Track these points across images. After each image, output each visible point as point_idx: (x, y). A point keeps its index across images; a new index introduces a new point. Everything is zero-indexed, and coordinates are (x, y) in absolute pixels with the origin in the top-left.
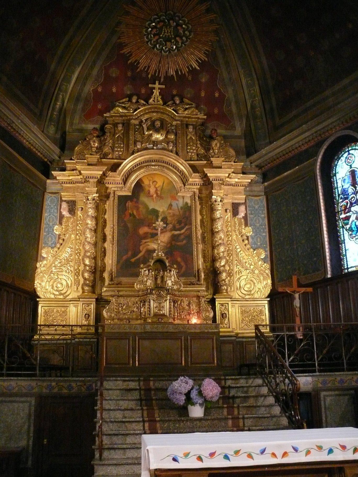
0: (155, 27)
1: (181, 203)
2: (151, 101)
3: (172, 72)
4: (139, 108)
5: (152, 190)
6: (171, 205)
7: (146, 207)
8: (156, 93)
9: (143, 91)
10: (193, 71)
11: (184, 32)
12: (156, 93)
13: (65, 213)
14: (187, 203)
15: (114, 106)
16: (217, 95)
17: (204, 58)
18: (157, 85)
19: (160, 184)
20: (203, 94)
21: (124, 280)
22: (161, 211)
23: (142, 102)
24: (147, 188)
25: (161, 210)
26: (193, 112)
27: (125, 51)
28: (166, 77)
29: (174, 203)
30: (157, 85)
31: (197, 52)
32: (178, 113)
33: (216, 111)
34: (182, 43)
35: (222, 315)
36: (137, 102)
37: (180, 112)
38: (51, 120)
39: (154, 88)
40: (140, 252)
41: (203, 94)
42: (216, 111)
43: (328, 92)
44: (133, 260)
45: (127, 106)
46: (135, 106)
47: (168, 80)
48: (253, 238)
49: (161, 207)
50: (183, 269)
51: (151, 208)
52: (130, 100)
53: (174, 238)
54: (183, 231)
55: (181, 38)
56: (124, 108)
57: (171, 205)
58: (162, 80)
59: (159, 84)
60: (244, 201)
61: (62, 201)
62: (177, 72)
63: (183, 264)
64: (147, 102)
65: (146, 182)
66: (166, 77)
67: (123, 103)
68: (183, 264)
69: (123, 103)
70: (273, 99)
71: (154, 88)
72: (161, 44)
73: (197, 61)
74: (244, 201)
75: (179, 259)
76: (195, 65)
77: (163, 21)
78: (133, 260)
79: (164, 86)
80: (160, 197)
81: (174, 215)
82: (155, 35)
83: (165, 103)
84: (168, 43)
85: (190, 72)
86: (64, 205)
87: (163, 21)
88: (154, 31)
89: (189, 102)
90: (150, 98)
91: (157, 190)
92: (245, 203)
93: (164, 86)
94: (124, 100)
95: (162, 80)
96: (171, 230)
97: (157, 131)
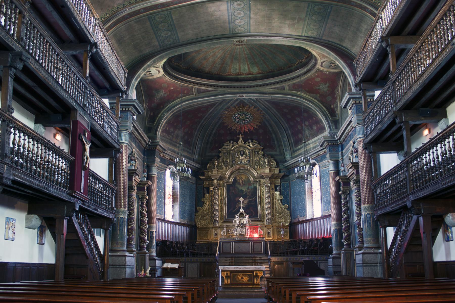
0: (237, 117)
1: (253, 186)
2: (239, 142)
3: (246, 130)
4: (234, 146)
5: (241, 182)
6: (248, 188)
7: (238, 189)
8: (241, 139)
9: (235, 138)
10: (255, 129)
11: (249, 117)
12: (241, 139)
13: (206, 192)
14: (255, 186)
15: (223, 145)
16: (268, 137)
17: (259, 124)
18: (241, 136)
19: (244, 179)
20: (261, 138)
21: (230, 219)
22: (244, 190)
23: (235, 143)
24: (238, 181)
25: (244, 190)
26: (257, 145)
27: (226, 124)
28: (244, 132)
29: (250, 187)
30: (241, 136)
31: (256, 123)
32: (250, 147)
33: (268, 144)
34: (249, 120)
35: (268, 233)
36: (233, 143)
37: (251, 145)
38: (197, 153)
39: (240, 137)
40: (236, 208)
41: (261, 138)
42: (268, 144)
43: (310, 141)
44: (233, 211)
45: (229, 145)
46: (231, 145)
47: (245, 134)
48: (283, 200)
49: (244, 189)
50: (254, 214)
51: (240, 189)
52: (230, 143)
53: (250, 202)
54: (253, 199)
55: (248, 119)
56: (228, 146)
57: (248, 188)
58: (243, 133)
59: (242, 135)
60: (280, 184)
61: (204, 188)
62: (249, 130)
63: (253, 212)
64: (237, 142)
65: (238, 178)
66: (244, 132)
67: (227, 144)
68: (253, 212)
69: (227, 144)
70: (292, 139)
71: (240, 137)
72: (240, 121)
73: (257, 125)
74: (280, 184)
75: (252, 210)
76: (256, 127)
77: (240, 115)
78: (233, 211)
79: (243, 136)
80: (244, 185)
81: (250, 192)
82: (237, 119)
83: (244, 143)
84: (243, 121)
85: (254, 130)
86: (205, 189)
87: (240, 115)
88: (237, 118)
89: (255, 141)
90: (238, 141)
91: (242, 182)
92: (280, 186)
93: (243, 136)
94: (227, 142)
95: (243, 133)
96: (249, 198)
97: (242, 156)
